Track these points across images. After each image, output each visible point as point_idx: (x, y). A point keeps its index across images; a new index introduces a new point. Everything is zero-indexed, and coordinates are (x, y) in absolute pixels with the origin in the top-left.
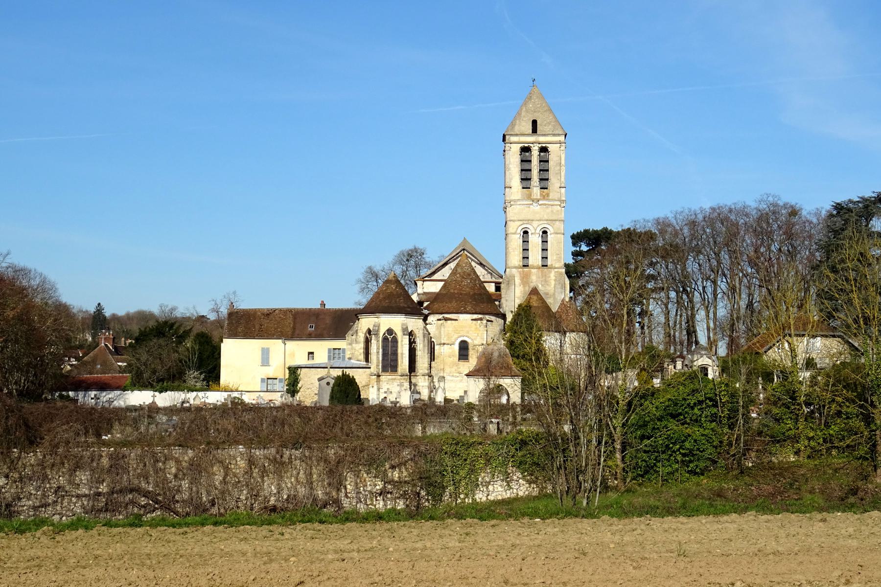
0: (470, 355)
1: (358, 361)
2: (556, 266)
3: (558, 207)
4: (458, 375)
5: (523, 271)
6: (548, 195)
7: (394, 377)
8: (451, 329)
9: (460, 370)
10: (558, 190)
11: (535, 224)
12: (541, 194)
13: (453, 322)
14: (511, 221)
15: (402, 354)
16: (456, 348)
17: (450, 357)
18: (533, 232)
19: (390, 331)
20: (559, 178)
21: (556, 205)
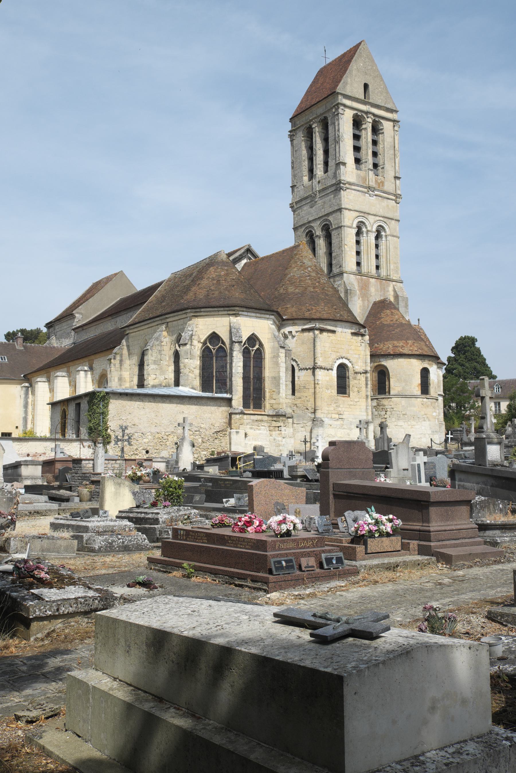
0: (351, 386)
1: (193, 388)
2: (394, 278)
3: (394, 202)
4: (337, 416)
5: (362, 280)
6: (382, 183)
7: (259, 417)
8: (327, 345)
9: (340, 409)
10: (393, 180)
11: (372, 219)
12: (376, 181)
13: (330, 334)
14: (346, 209)
15: (276, 380)
16: (334, 373)
17: (328, 389)
18: (369, 228)
19: (253, 339)
20: (393, 165)
21: (392, 199)
